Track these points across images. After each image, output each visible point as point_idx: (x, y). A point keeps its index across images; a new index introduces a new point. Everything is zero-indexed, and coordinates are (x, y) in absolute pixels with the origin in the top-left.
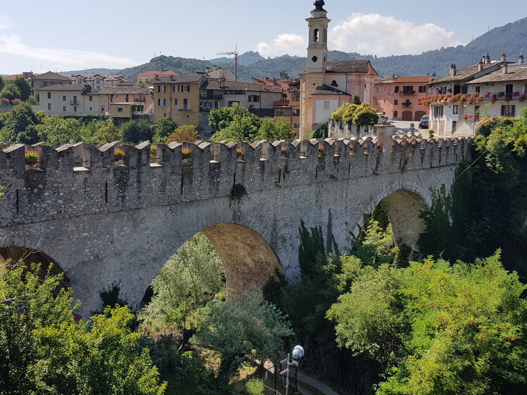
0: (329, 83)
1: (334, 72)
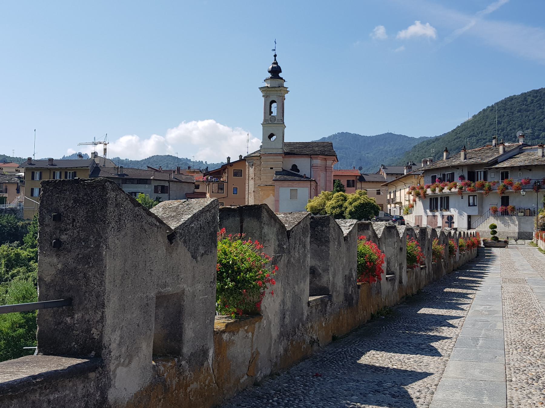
0: (289, 168)
1: (294, 154)
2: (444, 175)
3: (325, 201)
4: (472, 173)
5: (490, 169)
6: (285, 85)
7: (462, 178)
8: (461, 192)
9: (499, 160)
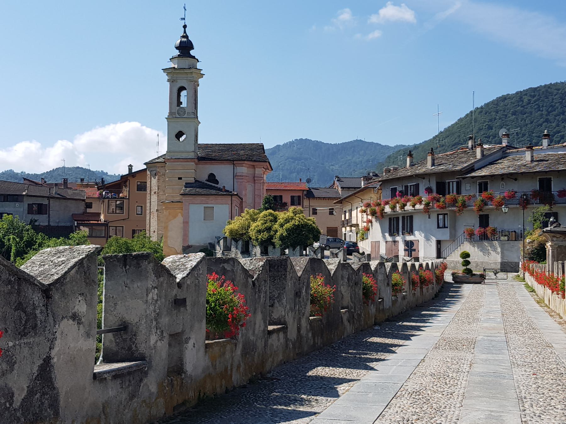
0: (204, 177)
2: (406, 187)
3: (249, 223)
4: (442, 184)
5: (464, 178)
6: (199, 66)
7: (429, 190)
8: (427, 209)
9: (476, 166)
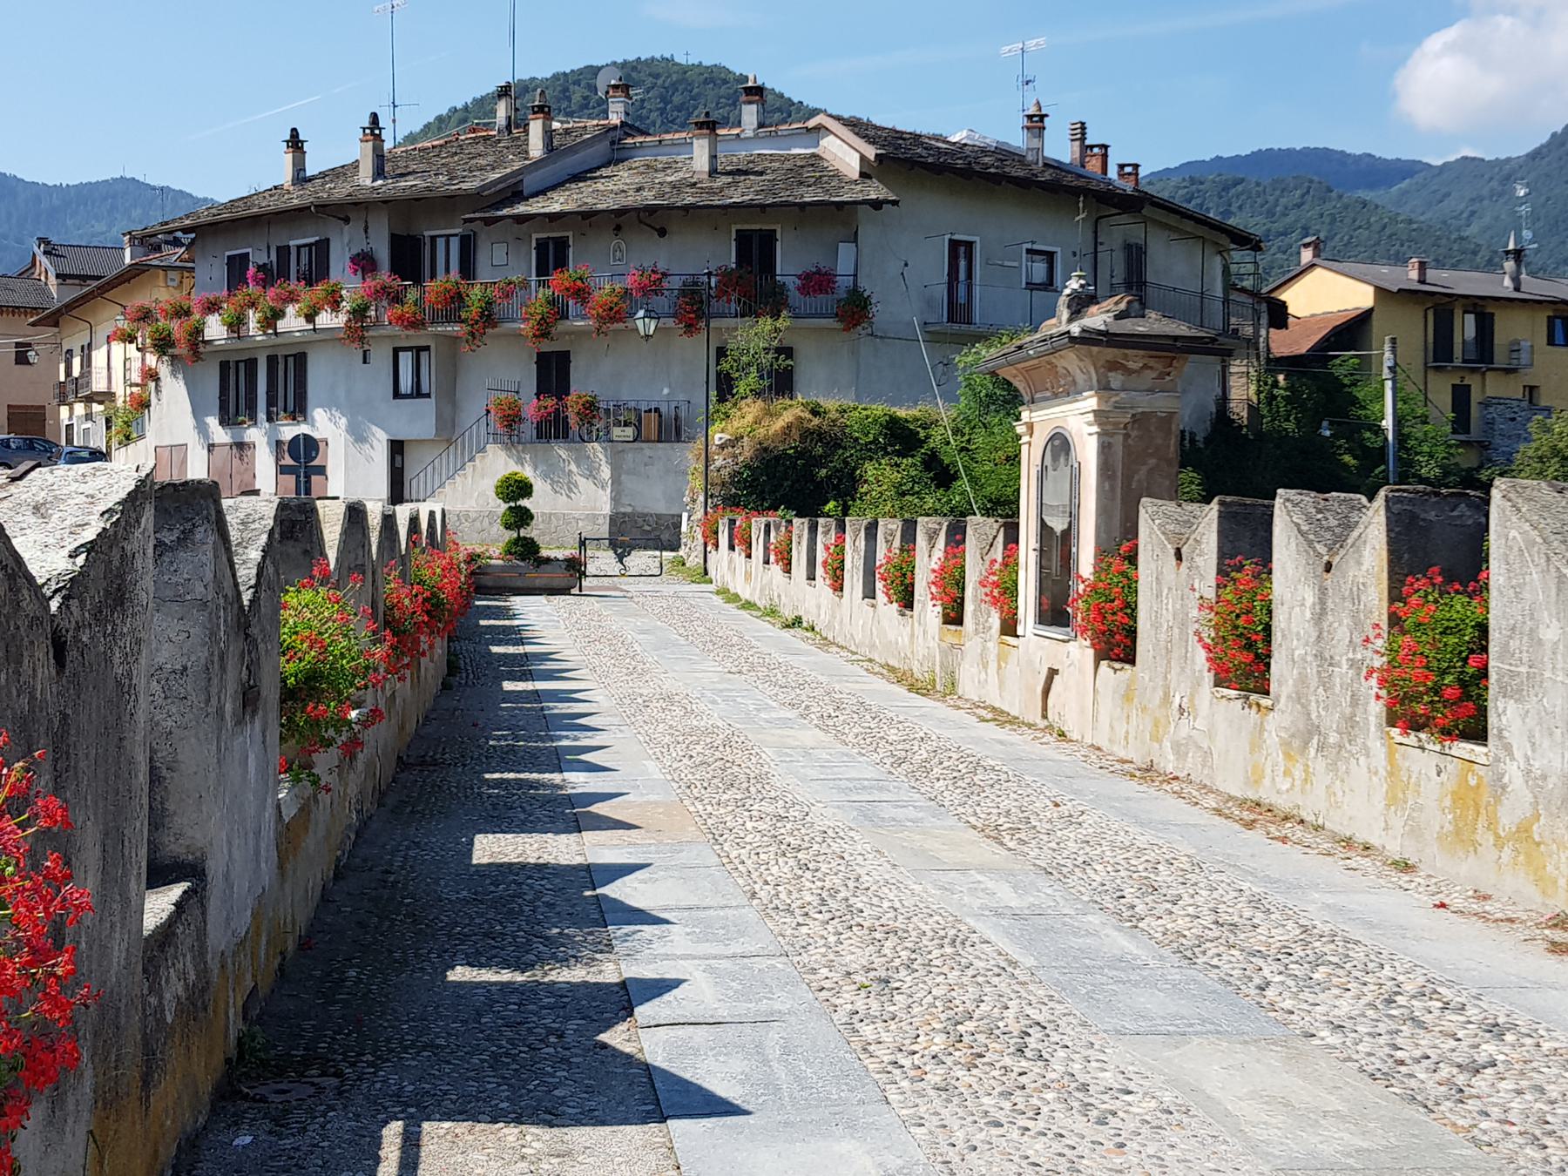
2: (284, 252)
5: (489, 222)
7: (364, 263)
